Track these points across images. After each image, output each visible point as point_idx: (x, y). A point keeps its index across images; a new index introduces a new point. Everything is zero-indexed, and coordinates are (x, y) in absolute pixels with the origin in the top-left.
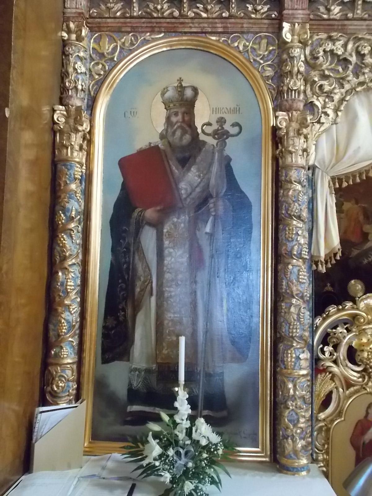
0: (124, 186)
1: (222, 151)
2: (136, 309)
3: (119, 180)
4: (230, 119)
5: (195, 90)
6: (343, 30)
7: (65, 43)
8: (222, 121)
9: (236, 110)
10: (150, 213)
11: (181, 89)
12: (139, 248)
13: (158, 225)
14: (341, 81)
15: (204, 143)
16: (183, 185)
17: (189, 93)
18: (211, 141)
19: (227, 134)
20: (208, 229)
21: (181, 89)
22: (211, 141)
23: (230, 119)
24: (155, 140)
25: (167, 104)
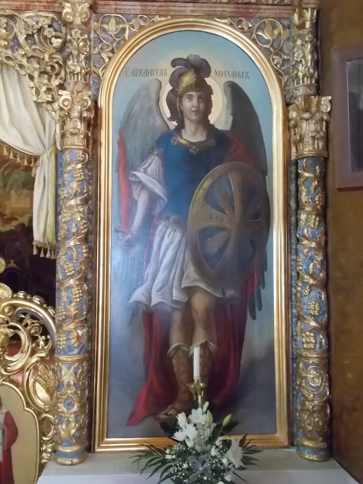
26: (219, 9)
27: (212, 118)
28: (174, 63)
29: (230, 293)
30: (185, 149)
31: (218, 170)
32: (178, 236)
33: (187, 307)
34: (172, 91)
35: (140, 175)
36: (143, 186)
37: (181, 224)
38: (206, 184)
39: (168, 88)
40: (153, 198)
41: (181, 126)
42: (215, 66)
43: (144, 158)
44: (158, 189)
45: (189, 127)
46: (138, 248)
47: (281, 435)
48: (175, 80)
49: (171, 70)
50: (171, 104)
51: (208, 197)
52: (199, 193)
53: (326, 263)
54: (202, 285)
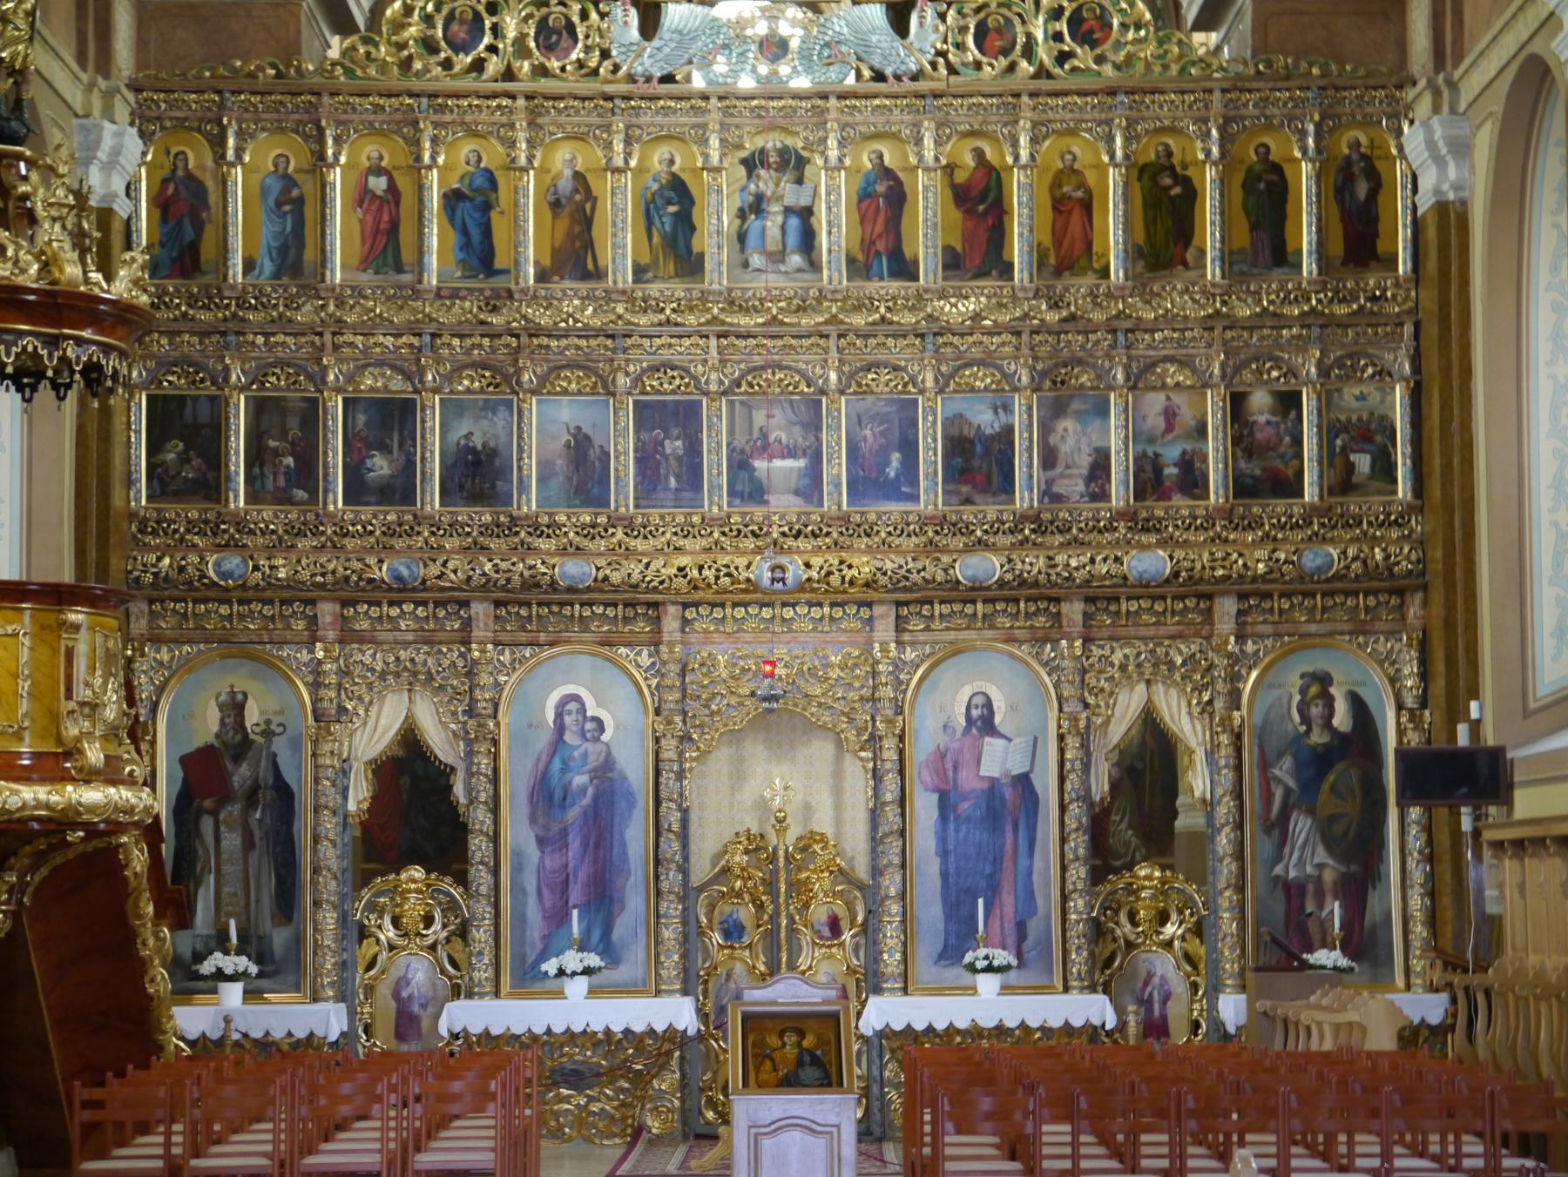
0: (185, 781)
1: (269, 747)
2: (198, 885)
3: (180, 774)
4: (276, 720)
5: (245, 695)
6: (373, 641)
7: (130, 661)
8: (268, 722)
9: (281, 712)
10: (208, 803)
11: (233, 693)
12: (199, 834)
13: (215, 813)
14: (370, 686)
15: (253, 741)
16: (235, 778)
17: (240, 697)
18: (259, 739)
19: (274, 734)
20: (258, 816)
21: (233, 693)
22: (259, 739)
23: (276, 720)
24: (211, 739)
25: (221, 707)
26: (1340, 627)
27: (1336, 722)
28: (1302, 676)
29: (1353, 868)
30: (1313, 748)
31: (1340, 766)
32: (1309, 822)
33: (1319, 879)
34: (1301, 701)
35: (1276, 772)
36: (1279, 781)
37: (1311, 812)
38: (1331, 777)
39: (1297, 698)
40: (1288, 791)
41: (1309, 730)
42: (1336, 677)
43: (1280, 756)
44: (1292, 783)
45: (1316, 730)
46: (1276, 832)
47: (1400, 982)
48: (1303, 691)
49: (1299, 683)
50: (1300, 711)
51: (1333, 789)
52: (1326, 786)
53: (1430, 842)
54: (1330, 861)
